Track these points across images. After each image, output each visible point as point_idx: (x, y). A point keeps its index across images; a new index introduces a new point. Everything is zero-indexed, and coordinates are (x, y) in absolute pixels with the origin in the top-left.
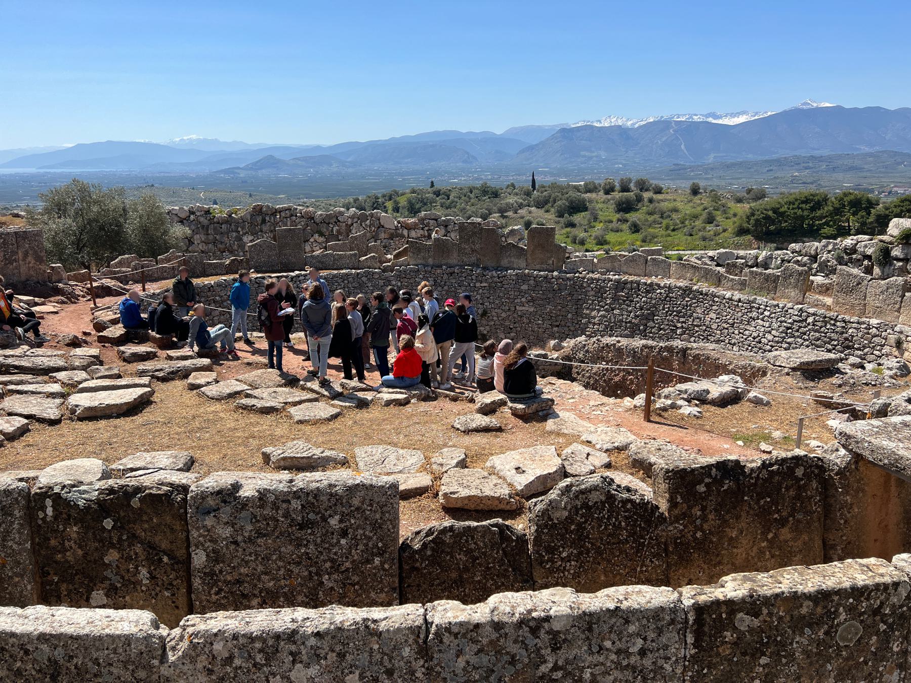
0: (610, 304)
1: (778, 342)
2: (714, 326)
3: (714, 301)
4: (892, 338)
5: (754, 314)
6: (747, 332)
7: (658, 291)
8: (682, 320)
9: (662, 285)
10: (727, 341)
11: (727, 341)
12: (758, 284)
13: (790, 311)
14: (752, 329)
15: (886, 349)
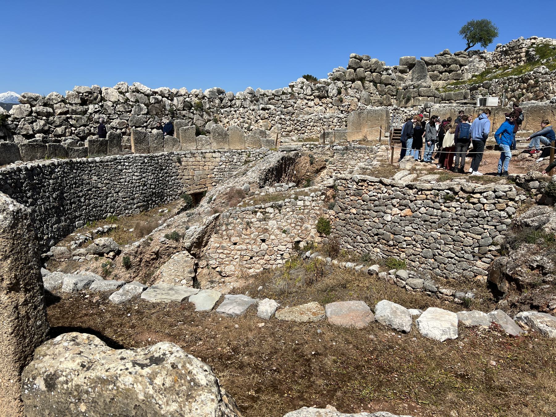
0: (32, 195)
1: (140, 179)
2: (100, 185)
3: (91, 167)
4: (175, 158)
5: (120, 167)
6: (123, 180)
7: (56, 170)
8: (79, 189)
9: (56, 163)
10: (113, 192)
11: (113, 192)
12: (96, 149)
13: (137, 158)
14: (124, 177)
15: (174, 164)
